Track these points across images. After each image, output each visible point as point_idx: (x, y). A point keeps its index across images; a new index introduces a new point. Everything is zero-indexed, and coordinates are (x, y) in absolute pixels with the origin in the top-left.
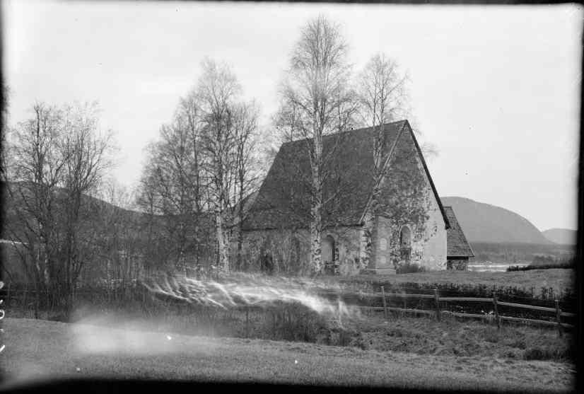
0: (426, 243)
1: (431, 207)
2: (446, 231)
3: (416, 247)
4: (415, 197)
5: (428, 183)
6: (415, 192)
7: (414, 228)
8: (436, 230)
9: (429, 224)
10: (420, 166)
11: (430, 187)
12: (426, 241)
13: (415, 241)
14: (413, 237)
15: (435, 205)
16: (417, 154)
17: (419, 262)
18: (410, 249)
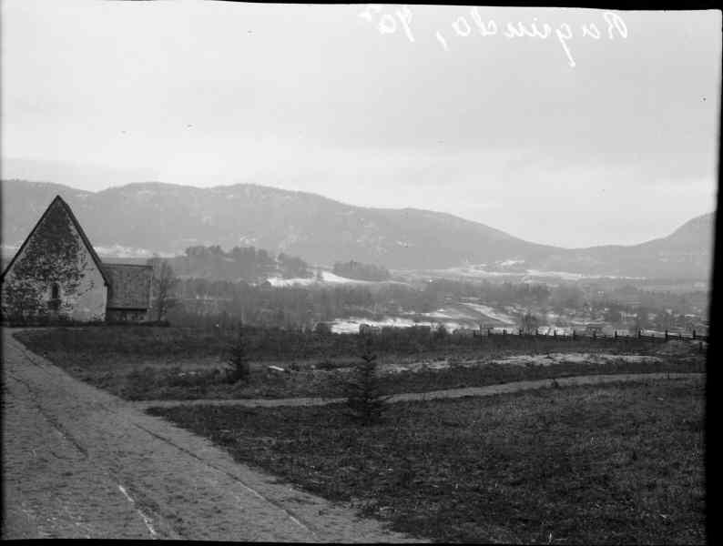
1: (87, 267)
3: (64, 299)
10: (75, 232)
15: (91, 264)
16: (71, 222)
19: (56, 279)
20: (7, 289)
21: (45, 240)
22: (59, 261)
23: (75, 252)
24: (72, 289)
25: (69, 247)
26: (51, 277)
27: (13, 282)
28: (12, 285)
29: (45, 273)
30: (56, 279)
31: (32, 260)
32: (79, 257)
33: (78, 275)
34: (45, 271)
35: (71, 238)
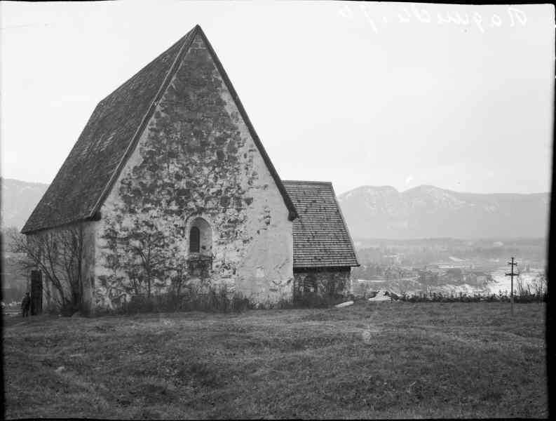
0: (247, 246)
1: (255, 183)
2: (291, 224)
3: (219, 251)
4: (219, 166)
5: (250, 140)
6: (220, 155)
7: (220, 221)
8: (268, 223)
9: (252, 214)
11: (255, 147)
12: (245, 242)
13: (220, 244)
14: (215, 237)
15: (264, 178)
16: (223, 85)
17: (231, 281)
18: (211, 259)
19: (201, 210)
20: (107, 236)
21: (177, 125)
22: (206, 170)
23: (235, 151)
24: (231, 230)
25: (220, 141)
26: (191, 205)
27: (119, 219)
28: (117, 227)
29: (182, 197)
30: (201, 210)
31: (155, 168)
33: (242, 201)
34: (181, 192)
35: (223, 120)
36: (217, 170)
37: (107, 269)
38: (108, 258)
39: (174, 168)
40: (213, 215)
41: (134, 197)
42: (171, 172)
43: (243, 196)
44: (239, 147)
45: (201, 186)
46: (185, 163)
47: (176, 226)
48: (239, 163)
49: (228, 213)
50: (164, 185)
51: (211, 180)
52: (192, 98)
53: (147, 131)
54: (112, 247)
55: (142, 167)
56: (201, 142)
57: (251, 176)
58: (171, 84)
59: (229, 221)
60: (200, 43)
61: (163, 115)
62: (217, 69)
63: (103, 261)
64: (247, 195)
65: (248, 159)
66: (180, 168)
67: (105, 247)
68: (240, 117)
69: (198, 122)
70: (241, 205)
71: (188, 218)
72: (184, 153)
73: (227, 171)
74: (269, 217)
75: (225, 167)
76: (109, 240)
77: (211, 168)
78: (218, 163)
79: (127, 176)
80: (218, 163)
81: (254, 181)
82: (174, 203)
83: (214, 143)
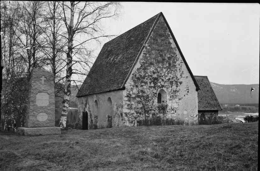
0: (180, 101)
1: (183, 76)
2: (197, 93)
3: (170, 104)
4: (169, 69)
5: (181, 58)
6: (170, 64)
7: (170, 90)
9: (182, 88)
10: (173, 45)
11: (183, 61)
13: (170, 100)
15: (186, 73)
16: (171, 37)
18: (167, 106)
19: (163, 86)
20: (127, 96)
21: (153, 52)
22: (164, 70)
25: (169, 58)
26: (159, 84)
28: (131, 93)
29: (155, 80)
30: (163, 86)
31: (145, 69)
32: (178, 66)
35: (170, 49)
36: (168, 70)
37: (128, 110)
38: (128, 105)
39: (152, 69)
40: (167, 88)
41: (137, 81)
42: (151, 70)
43: (178, 81)
44: (177, 61)
45: (162, 76)
46: (156, 67)
47: (153, 92)
48: (177, 68)
49: (172, 87)
50: (149, 75)
51: (166, 74)
52: (159, 41)
53: (142, 54)
54: (129, 101)
55: (140, 68)
56: (162, 59)
57: (181, 73)
58: (151, 35)
59: (173, 91)
60: (162, 20)
61: (148, 48)
62: (168, 30)
63: (126, 106)
64: (180, 80)
65: (180, 66)
66: (154, 69)
67: (127, 101)
68: (177, 49)
69: (161, 51)
70: (178, 84)
71: (158, 89)
72: (156, 63)
73: (172, 70)
74: (188, 89)
75: (172, 69)
76: (128, 98)
77: (166, 69)
78: (169, 68)
79: (134, 72)
80: (169, 68)
81: (183, 75)
82: (152, 83)
83: (167, 59)
